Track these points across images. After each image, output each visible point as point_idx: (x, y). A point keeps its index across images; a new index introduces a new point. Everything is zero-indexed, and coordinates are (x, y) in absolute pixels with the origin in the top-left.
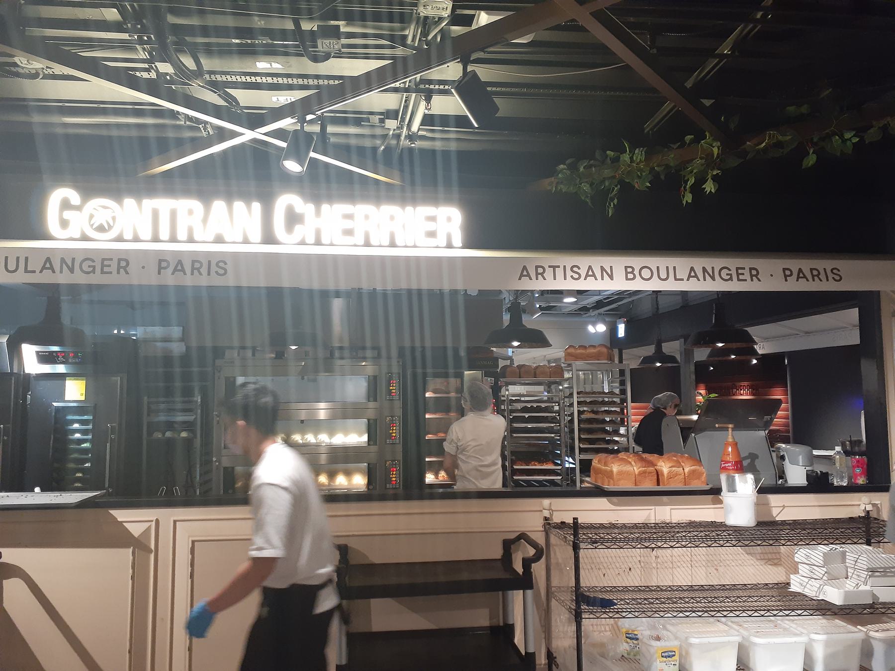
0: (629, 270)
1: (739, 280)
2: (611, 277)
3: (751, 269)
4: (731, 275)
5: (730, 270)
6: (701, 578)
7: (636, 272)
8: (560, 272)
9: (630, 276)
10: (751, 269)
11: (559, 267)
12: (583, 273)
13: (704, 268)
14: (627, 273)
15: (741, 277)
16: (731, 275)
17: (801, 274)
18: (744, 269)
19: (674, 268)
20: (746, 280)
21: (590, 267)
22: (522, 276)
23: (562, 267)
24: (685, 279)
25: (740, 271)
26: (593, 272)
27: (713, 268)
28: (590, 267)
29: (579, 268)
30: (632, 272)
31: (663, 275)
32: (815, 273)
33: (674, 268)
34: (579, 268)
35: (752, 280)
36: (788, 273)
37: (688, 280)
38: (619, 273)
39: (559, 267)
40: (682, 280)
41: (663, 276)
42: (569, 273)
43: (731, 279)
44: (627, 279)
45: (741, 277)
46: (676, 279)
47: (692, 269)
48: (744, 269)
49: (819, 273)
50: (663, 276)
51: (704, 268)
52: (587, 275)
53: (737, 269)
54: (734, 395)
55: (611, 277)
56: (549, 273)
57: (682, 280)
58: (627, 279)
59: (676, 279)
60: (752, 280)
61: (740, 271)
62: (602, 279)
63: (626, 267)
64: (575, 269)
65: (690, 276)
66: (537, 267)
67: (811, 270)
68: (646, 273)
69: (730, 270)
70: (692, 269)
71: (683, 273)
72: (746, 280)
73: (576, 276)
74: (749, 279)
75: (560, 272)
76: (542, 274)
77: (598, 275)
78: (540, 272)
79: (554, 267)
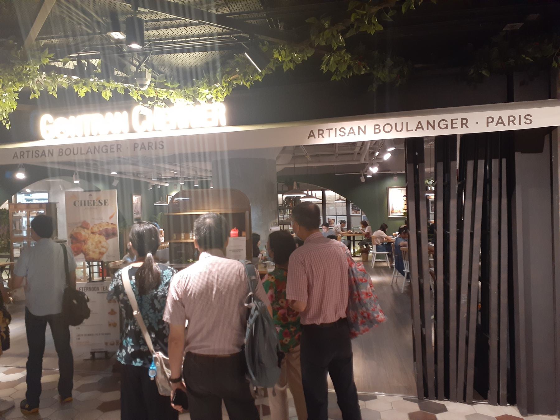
0: (377, 127)
1: (452, 128)
2: (364, 133)
4: (447, 125)
5: (446, 121)
6: (442, 341)
7: (381, 128)
9: (377, 131)
10: (462, 119)
14: (375, 129)
15: (454, 126)
18: (457, 119)
19: (407, 123)
20: (457, 128)
21: (352, 128)
22: (310, 136)
24: (414, 129)
25: (454, 122)
27: (434, 121)
28: (352, 128)
31: (399, 128)
33: (407, 123)
34: (345, 129)
35: (462, 127)
40: (412, 130)
43: (447, 128)
44: (375, 133)
45: (454, 126)
47: (420, 123)
48: (457, 119)
50: (399, 129)
53: (452, 120)
54: (165, 297)
55: (364, 133)
56: (326, 133)
58: (375, 133)
60: (462, 127)
61: (454, 122)
65: (417, 128)
68: (388, 128)
69: (446, 121)
70: (420, 123)
71: (413, 126)
72: (457, 128)
76: (322, 134)
78: (321, 133)
79: (329, 130)
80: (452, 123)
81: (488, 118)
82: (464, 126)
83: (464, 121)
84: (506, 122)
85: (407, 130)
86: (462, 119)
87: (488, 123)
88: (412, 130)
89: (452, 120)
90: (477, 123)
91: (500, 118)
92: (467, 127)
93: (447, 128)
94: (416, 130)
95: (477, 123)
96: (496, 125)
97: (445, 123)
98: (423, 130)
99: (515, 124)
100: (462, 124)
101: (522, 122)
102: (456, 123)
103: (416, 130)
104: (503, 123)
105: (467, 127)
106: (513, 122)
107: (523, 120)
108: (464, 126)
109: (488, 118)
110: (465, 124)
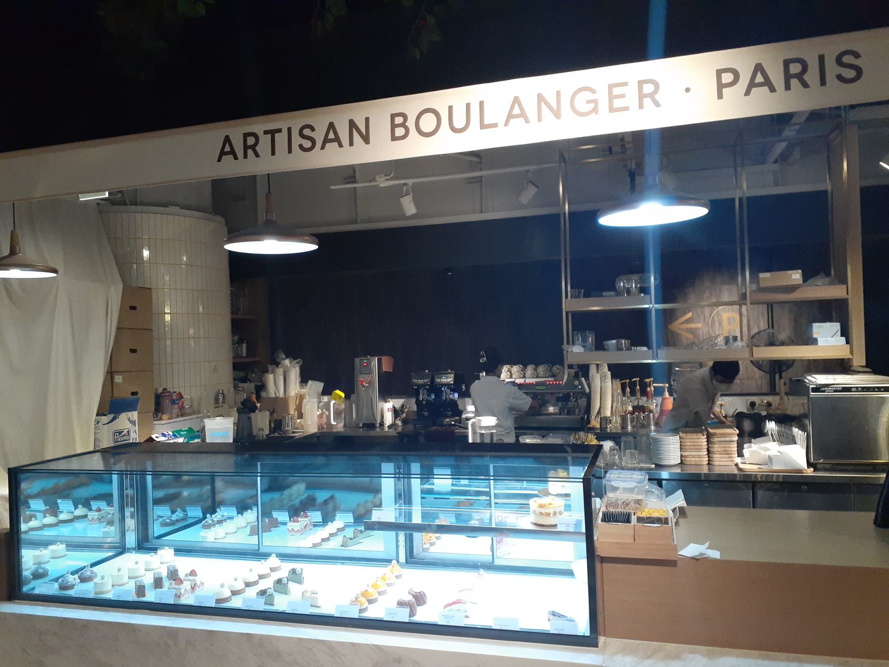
1: (612, 109)
4: (595, 102)
5: (593, 91)
8: (281, 139)
10: (641, 83)
11: (280, 131)
14: (394, 126)
15: (617, 103)
16: (595, 102)
18: (625, 84)
19: (482, 104)
20: (626, 109)
24: (501, 121)
25: (616, 91)
26: (335, 133)
29: (312, 129)
30: (403, 125)
35: (641, 106)
39: (280, 131)
42: (297, 140)
43: (595, 110)
44: (394, 138)
45: (617, 103)
48: (625, 84)
52: (326, 141)
53: (611, 87)
58: (394, 138)
60: (641, 106)
61: (616, 91)
64: (307, 132)
65: (510, 116)
66: (246, 136)
69: (593, 91)
72: (626, 109)
73: (307, 144)
80: (611, 97)
82: (647, 101)
83: (648, 88)
85: (483, 126)
86: (641, 83)
87: (721, 86)
88: (494, 125)
89: (611, 87)
90: (688, 90)
92: (657, 104)
93: (595, 110)
94: (506, 124)
95: (688, 90)
96: (747, 93)
97: (588, 95)
98: (527, 121)
100: (642, 96)
101: (830, 76)
102: (623, 96)
103: (506, 124)
105: (657, 104)
108: (647, 101)
110: (651, 96)
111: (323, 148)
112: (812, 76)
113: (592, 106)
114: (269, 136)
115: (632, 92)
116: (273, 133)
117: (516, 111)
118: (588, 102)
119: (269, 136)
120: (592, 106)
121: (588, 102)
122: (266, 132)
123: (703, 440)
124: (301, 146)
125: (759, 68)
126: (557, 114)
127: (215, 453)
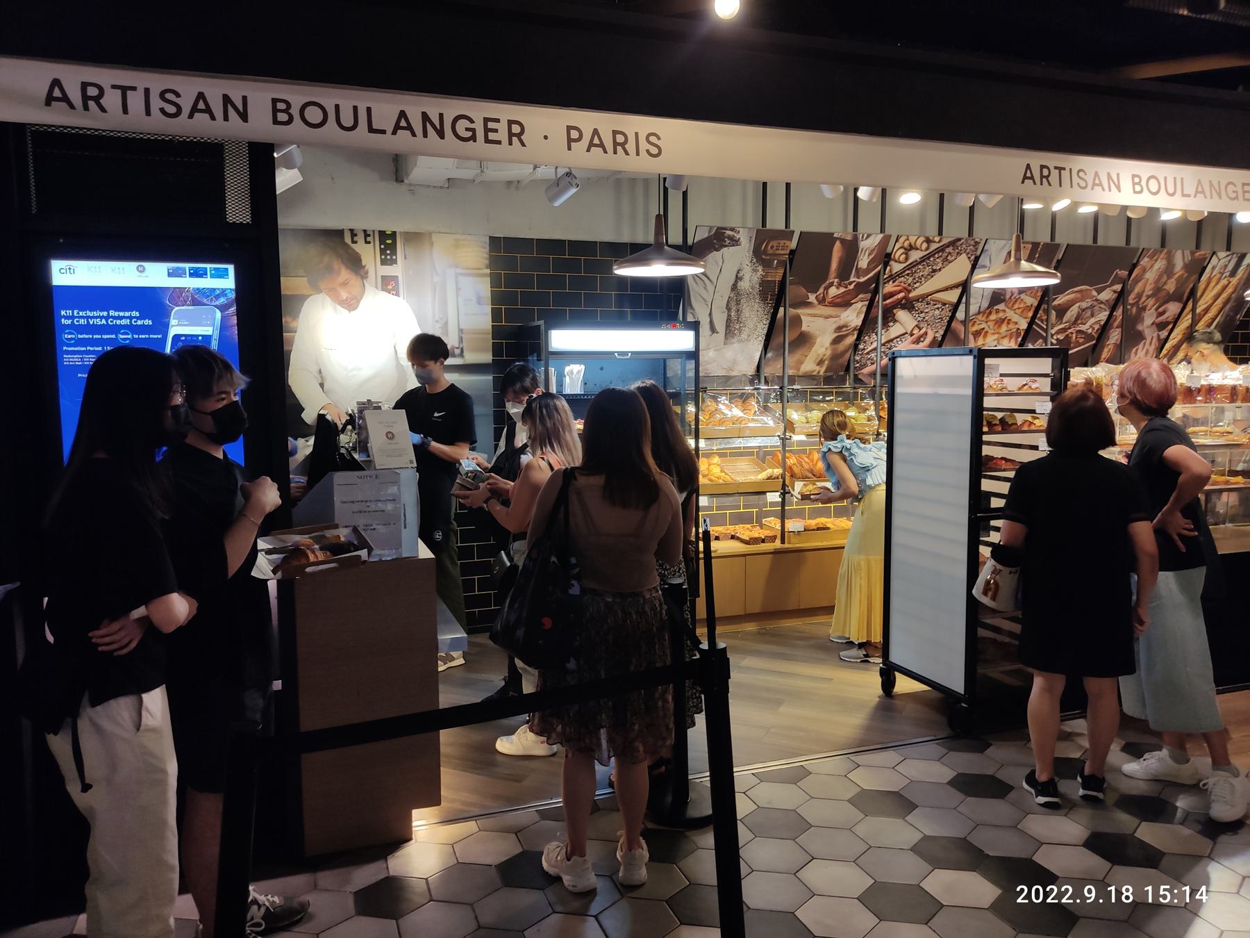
0: (281, 106)
1: (487, 141)
2: (244, 116)
3: (510, 123)
4: (473, 130)
5: (472, 121)
7: (295, 111)
9: (282, 117)
10: (510, 123)
11: (134, 89)
12: (186, 104)
13: (424, 115)
14: (275, 111)
15: (492, 136)
16: (473, 130)
17: (596, 142)
18: (497, 121)
20: (499, 142)
23: (140, 94)
25: (491, 125)
27: (441, 115)
29: (178, 95)
30: (286, 111)
31: (347, 121)
32: (620, 139)
33: (369, 110)
36: (574, 134)
37: (394, 133)
38: (1126, 184)
39: (134, 89)
40: (383, 132)
41: (1171, 190)
44: (276, 122)
45: (492, 136)
46: (371, 130)
47: (403, 114)
48: (497, 121)
49: (626, 141)
50: (347, 121)
51: (424, 115)
52: (195, 109)
53: (486, 120)
55: (244, 116)
57: (383, 132)
58: (276, 122)
59: (371, 130)
60: (510, 143)
61: (491, 125)
62: (425, 135)
63: (275, 101)
67: (615, 133)
69: (472, 121)
70: (403, 114)
72: (499, 142)
73: (171, 109)
74: (505, 140)
75: (136, 100)
77: (418, 129)
80: (487, 130)
81: (569, 128)
84: (217, 109)
87: (570, 140)
89: (486, 120)
90: (546, 137)
91: (596, 132)
95: (546, 137)
96: (588, 150)
99: (627, 154)
100: (511, 135)
102: (496, 131)
103: (394, 133)
104: (208, 110)
106: (623, 145)
107: (156, 103)
108: (515, 139)
109: (569, 128)
111: (191, 116)
112: (631, 147)
113: (469, 134)
114: (119, 92)
115: (502, 127)
116: (124, 90)
117: (403, 123)
118: (467, 129)
119: (119, 92)
120: (469, 134)
121: (467, 129)
122: (114, 87)
123: (487, 357)
124: (162, 110)
125: (596, 132)
126: (441, 134)
127: (805, 610)
